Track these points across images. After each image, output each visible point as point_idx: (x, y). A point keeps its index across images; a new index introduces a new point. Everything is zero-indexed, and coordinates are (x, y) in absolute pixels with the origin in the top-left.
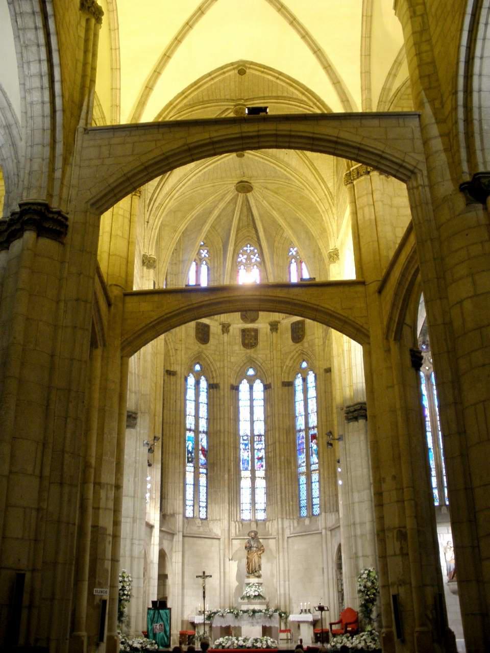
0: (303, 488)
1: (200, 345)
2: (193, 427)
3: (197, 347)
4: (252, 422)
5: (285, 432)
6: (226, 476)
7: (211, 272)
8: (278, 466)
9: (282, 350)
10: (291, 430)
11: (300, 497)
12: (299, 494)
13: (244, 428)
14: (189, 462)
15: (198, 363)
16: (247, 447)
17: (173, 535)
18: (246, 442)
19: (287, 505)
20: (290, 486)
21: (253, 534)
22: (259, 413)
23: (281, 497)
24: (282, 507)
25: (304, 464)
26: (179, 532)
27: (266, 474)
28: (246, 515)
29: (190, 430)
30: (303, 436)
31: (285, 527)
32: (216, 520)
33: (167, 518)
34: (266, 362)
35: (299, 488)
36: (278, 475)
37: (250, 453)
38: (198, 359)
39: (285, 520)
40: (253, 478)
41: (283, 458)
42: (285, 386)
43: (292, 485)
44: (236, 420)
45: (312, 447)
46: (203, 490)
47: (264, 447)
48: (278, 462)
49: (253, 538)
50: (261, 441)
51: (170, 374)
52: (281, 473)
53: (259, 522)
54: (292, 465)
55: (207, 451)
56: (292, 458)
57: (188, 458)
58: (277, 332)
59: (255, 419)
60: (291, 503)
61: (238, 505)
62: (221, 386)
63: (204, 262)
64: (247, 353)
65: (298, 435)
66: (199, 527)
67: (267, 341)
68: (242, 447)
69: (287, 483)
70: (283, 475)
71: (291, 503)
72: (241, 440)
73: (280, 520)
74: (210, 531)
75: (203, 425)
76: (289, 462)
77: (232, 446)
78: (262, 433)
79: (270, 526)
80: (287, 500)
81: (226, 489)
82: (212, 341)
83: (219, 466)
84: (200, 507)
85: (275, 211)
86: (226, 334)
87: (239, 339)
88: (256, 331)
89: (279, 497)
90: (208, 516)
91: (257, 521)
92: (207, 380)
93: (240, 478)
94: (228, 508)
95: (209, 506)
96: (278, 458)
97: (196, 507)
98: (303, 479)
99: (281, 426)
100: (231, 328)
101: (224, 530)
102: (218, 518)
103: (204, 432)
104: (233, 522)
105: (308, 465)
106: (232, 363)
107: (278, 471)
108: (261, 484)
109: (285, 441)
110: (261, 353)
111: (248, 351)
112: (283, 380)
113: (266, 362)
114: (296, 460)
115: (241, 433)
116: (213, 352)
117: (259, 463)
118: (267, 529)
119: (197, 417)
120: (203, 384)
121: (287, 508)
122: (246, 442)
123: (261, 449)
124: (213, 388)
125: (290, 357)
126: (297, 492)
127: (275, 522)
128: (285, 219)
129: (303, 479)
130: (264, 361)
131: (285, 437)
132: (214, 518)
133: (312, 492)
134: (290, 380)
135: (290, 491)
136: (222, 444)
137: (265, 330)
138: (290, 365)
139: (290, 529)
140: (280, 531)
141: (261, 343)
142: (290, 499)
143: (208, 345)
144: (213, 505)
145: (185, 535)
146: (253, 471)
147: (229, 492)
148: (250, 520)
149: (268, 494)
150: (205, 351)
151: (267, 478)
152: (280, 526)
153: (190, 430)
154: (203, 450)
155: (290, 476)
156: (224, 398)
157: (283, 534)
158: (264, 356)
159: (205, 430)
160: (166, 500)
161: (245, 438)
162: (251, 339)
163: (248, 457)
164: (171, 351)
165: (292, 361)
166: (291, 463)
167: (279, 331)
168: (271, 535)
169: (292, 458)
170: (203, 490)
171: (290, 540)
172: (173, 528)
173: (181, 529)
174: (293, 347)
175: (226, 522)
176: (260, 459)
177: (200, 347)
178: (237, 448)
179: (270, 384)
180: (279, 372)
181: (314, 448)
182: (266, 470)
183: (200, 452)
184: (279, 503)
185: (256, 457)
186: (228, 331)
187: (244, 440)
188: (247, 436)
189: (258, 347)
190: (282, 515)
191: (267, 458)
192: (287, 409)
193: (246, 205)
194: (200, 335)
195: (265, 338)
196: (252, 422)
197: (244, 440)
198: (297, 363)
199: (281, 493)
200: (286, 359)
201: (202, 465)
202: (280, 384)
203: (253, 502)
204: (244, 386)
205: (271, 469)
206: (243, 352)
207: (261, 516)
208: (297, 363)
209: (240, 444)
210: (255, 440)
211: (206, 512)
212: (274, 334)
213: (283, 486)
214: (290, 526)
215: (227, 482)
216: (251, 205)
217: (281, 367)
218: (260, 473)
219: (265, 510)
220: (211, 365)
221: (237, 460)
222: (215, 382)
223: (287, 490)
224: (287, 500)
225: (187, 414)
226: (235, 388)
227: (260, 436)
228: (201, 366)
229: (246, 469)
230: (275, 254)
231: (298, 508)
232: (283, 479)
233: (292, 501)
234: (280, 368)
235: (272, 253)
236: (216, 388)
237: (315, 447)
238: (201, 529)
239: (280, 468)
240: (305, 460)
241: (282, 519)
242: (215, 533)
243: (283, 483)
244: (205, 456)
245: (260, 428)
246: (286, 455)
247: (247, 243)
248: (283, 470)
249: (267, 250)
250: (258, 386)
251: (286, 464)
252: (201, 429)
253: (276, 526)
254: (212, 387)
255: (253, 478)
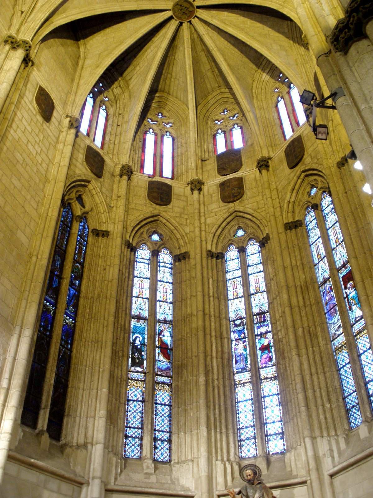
0: (347, 373)
1: (155, 206)
2: (145, 314)
3: (151, 209)
4: (248, 296)
5: (299, 289)
6: (202, 379)
7: (177, 143)
8: (293, 344)
9: (279, 188)
10: (311, 285)
11: (343, 391)
12: (341, 386)
13: (236, 308)
14: (134, 364)
15: (155, 232)
16: (243, 335)
17: (79, 484)
18: (240, 328)
19: (321, 411)
20: (321, 376)
21: (249, 472)
22: (257, 280)
23: (306, 398)
24: (310, 416)
25: (341, 331)
26: (93, 478)
27: (278, 371)
28: (249, 450)
29: (139, 318)
30: (331, 288)
31: (321, 454)
32: (186, 461)
33: (68, 450)
34: (259, 211)
35: (340, 375)
36: (295, 358)
37: (247, 343)
38: (151, 223)
39: (319, 439)
40: (256, 381)
41: (300, 330)
42: (291, 229)
43: (324, 373)
44: (222, 298)
45: (347, 296)
46: (163, 412)
47: (270, 329)
48: (292, 337)
49: (251, 482)
50: (265, 320)
51: (97, 235)
52: (299, 355)
53: (273, 459)
54: (320, 339)
55: (171, 349)
56: (319, 329)
57: (133, 359)
58: (268, 171)
59: (252, 290)
60: (328, 406)
61: (231, 431)
62: (192, 254)
63: (168, 134)
64: (229, 208)
65: (322, 290)
66: (148, 475)
67: (257, 186)
68: (234, 336)
69: (314, 371)
70: (304, 358)
71: (328, 406)
72: (232, 326)
73: (308, 441)
74: (173, 483)
75: (165, 311)
76: (313, 336)
77: (213, 334)
78: (266, 307)
79: (293, 458)
80: (319, 402)
81: (202, 401)
82: (176, 204)
83: (190, 368)
84: (155, 440)
85: (230, 26)
86: (196, 193)
87: (217, 196)
88: (240, 181)
89: (301, 396)
90: (174, 457)
91: (267, 458)
92: (171, 253)
93: (234, 386)
94: (205, 434)
95: (174, 438)
96: (291, 330)
97: (147, 440)
98: (343, 357)
99: (291, 283)
100: (205, 188)
101: (200, 477)
102: (190, 458)
103: (165, 321)
104: (219, 462)
105: (347, 326)
106: (209, 225)
107: (294, 352)
108: (270, 388)
109: (301, 303)
110: (248, 204)
111: (231, 205)
112: (285, 221)
113: (259, 211)
114: (325, 329)
115: (232, 316)
116: (178, 215)
117: (265, 356)
118: (288, 469)
119: (153, 300)
120: (165, 257)
121: (322, 417)
122: (240, 328)
123: (266, 333)
124: (179, 260)
125: (290, 188)
126: (337, 384)
127: (301, 450)
128: (247, 33)
129: (343, 357)
130: (255, 211)
131: (301, 298)
132: (183, 459)
133: (363, 372)
134: (297, 219)
135: (323, 385)
136: (194, 332)
137: (253, 176)
138: (292, 200)
139: (333, 457)
140: (312, 464)
141: (248, 191)
142: (325, 399)
143: (170, 206)
144: (182, 434)
145: (112, 486)
146: (256, 371)
147: (208, 407)
148: (255, 457)
149: (284, 403)
150: (163, 214)
151: (281, 376)
152: (310, 453)
153: (139, 318)
154: (164, 348)
155: (318, 359)
156: (195, 269)
157: (318, 468)
158: (255, 204)
159: (169, 318)
160: (71, 420)
161: (238, 322)
162: (232, 189)
163: (245, 349)
164: (100, 205)
165: (294, 194)
166: (317, 336)
167: (270, 169)
168: (296, 477)
169: (319, 329)
170: (163, 412)
171: (337, 480)
172: (78, 470)
173: (98, 474)
174: (292, 175)
175: (203, 462)
176: (265, 348)
177: (155, 209)
178: (222, 338)
179: (268, 234)
180: (278, 213)
181: (351, 296)
182: (277, 365)
183: (158, 350)
184: (303, 409)
185: (259, 346)
186: (200, 190)
187: (236, 325)
188: (241, 318)
189: (245, 197)
190: (312, 429)
191: (277, 341)
192: (299, 257)
193: (203, 50)
194: (155, 194)
195: (254, 184)
196: (248, 296)
197: (236, 325)
198: (303, 194)
199: (305, 390)
200: (286, 193)
201: (160, 369)
202: (281, 229)
203: (260, 423)
204: (232, 254)
205: (284, 358)
206: (224, 208)
207: (276, 446)
208: (303, 194)
209: (229, 332)
210: (255, 321)
211: (170, 449)
212: (264, 172)
213: (308, 378)
214: (331, 450)
215: (202, 388)
216: (201, 33)
217: (280, 207)
218: (268, 372)
219: (282, 433)
220: (175, 231)
221: (226, 359)
222: (183, 251)
223: (316, 383)
224: (319, 402)
225: (135, 294)
226: (220, 257)
227: (262, 313)
228: (160, 235)
229: (243, 370)
230: (255, 100)
231: (343, 413)
232: (306, 366)
233: (329, 401)
234: (279, 209)
235: (250, 97)
236: (184, 258)
237: (352, 293)
238: (153, 479)
239: (297, 347)
240: (340, 323)
241: (313, 438)
242: (183, 487)
243: (307, 372)
244: (167, 356)
245: (260, 302)
246: (306, 325)
247: (222, 107)
248: (303, 351)
249: (237, 86)
250: (253, 248)
251: (308, 341)
252: (159, 316)
253: (304, 458)
254: (180, 258)
255: (256, 381)
